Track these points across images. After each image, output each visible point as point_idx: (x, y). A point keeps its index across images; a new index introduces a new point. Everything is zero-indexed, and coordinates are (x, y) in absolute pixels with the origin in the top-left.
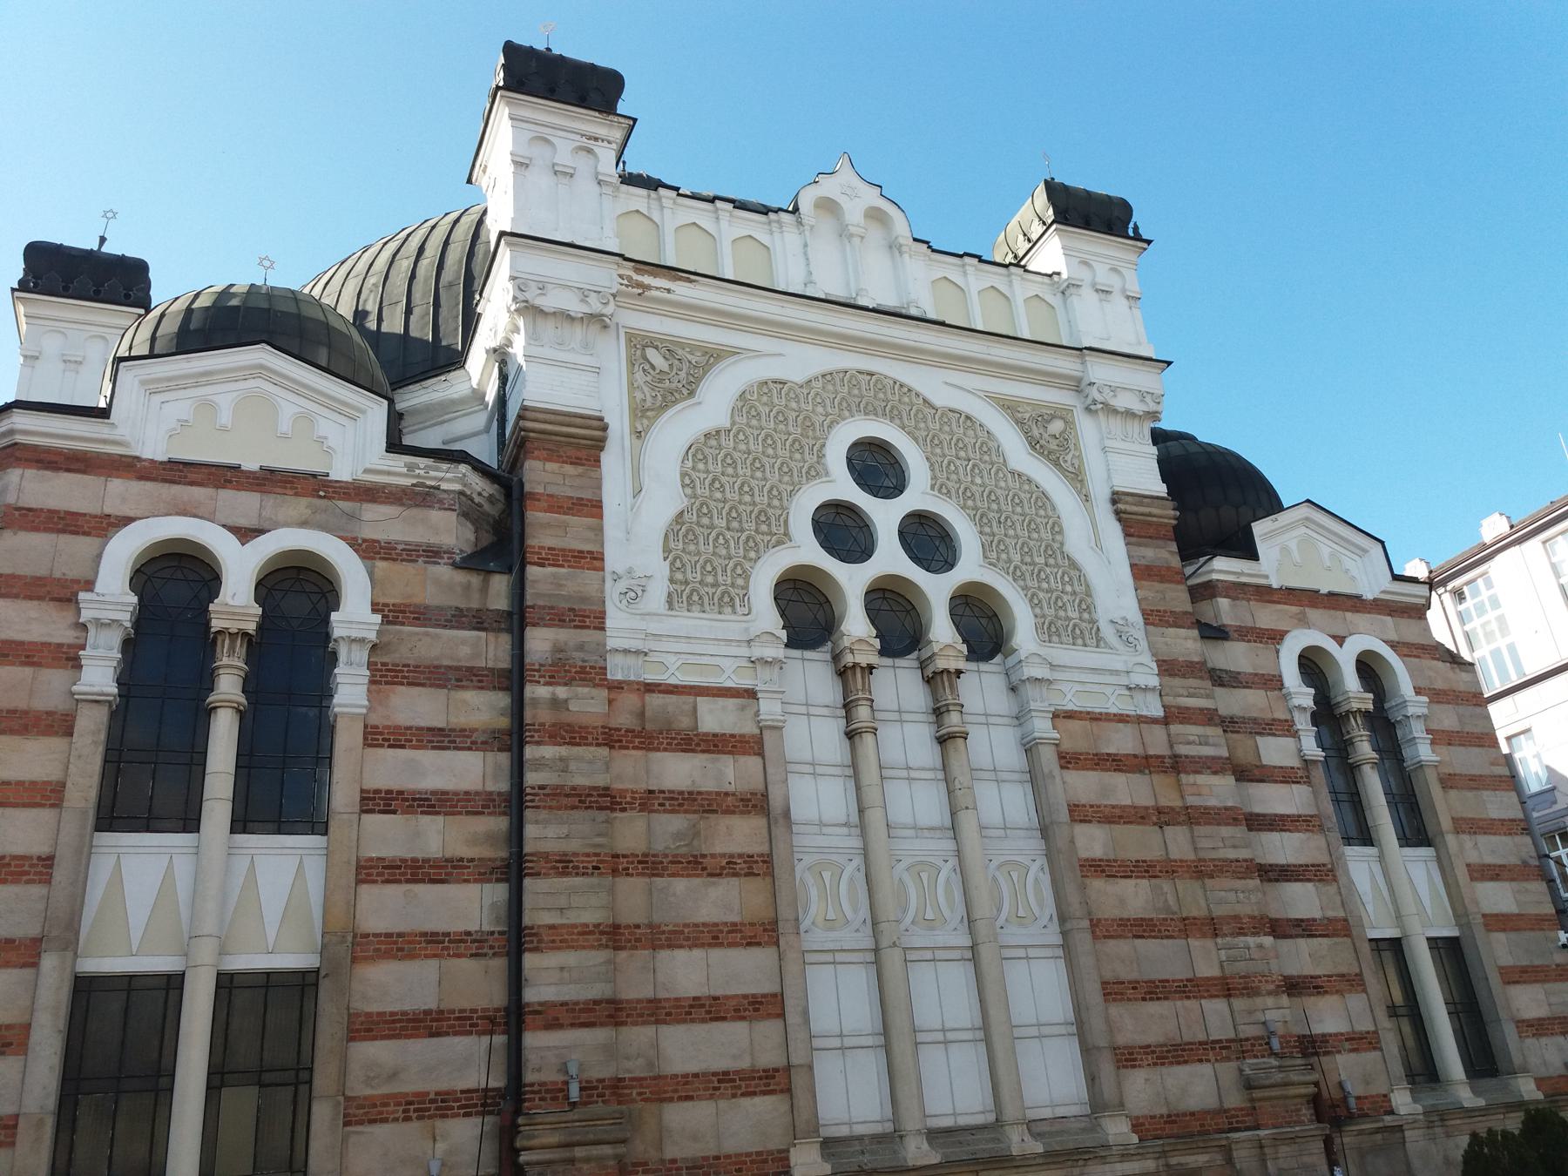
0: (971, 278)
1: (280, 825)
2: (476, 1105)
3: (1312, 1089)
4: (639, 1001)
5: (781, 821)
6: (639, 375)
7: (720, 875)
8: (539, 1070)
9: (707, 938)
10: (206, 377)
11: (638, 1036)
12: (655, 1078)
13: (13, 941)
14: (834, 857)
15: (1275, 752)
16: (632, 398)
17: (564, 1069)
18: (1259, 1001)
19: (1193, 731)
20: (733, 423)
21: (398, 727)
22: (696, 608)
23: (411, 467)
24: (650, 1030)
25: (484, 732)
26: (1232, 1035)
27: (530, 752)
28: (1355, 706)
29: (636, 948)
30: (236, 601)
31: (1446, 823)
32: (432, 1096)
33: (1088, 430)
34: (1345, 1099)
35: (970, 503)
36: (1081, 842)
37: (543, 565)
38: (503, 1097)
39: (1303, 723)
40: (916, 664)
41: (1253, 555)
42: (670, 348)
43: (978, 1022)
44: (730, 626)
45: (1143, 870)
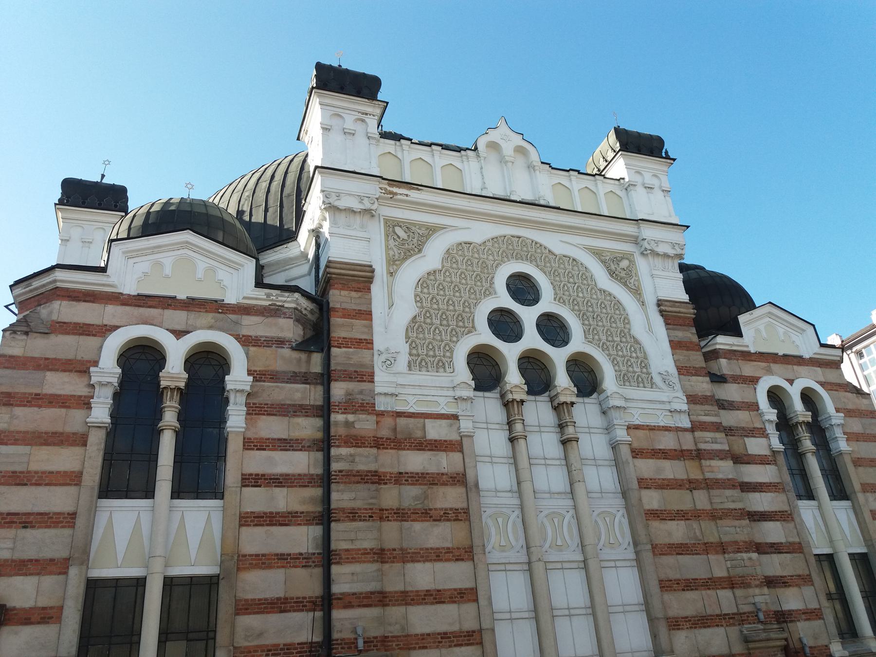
0: (574, 183)
1: (198, 494)
2: (306, 652)
3: (783, 643)
4: (396, 592)
5: (474, 489)
6: (391, 242)
7: (439, 520)
8: (341, 632)
9: (434, 557)
10: (158, 249)
11: (395, 612)
12: (405, 636)
13: (54, 560)
14: (504, 510)
15: (755, 446)
16: (387, 254)
17: (354, 631)
18: (751, 591)
19: (708, 435)
20: (443, 267)
21: (262, 439)
22: (424, 369)
23: (268, 295)
24: (402, 609)
25: (309, 440)
26: (735, 611)
27: (333, 451)
28: (801, 419)
29: (393, 562)
30: (174, 370)
31: (857, 487)
32: (281, 646)
33: (643, 266)
34: (803, 648)
35: (576, 307)
36: (645, 500)
37: (340, 347)
38: (321, 647)
39: (771, 430)
40: (548, 399)
41: (740, 335)
42: (408, 227)
43: (589, 604)
44: (442, 379)
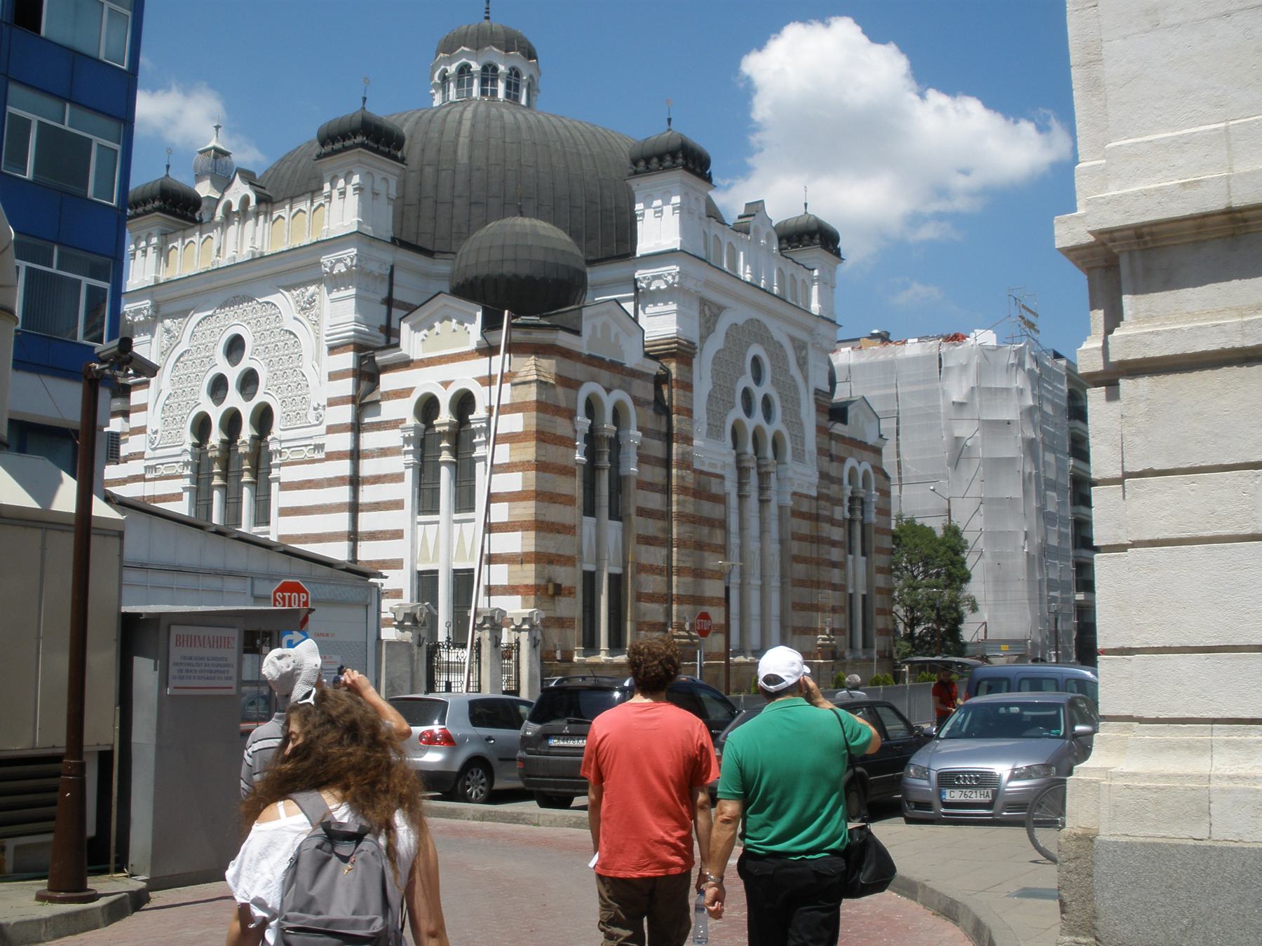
28: (861, 495)
45: (805, 560)
